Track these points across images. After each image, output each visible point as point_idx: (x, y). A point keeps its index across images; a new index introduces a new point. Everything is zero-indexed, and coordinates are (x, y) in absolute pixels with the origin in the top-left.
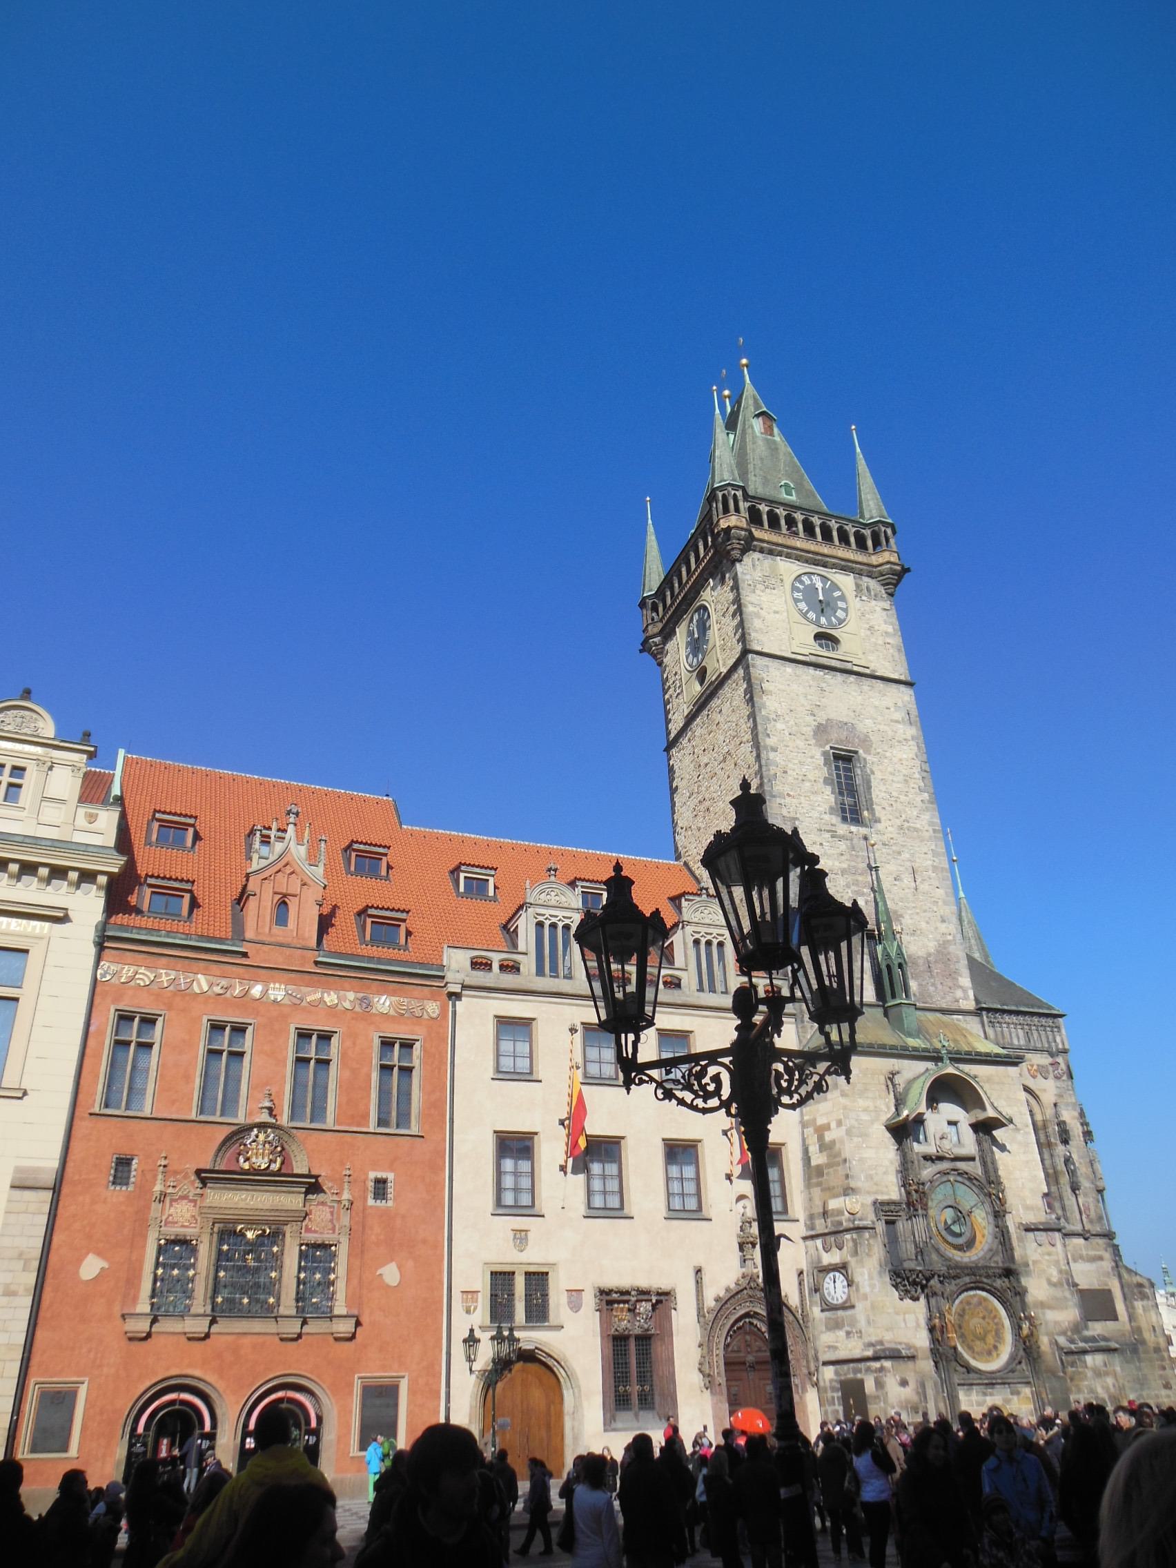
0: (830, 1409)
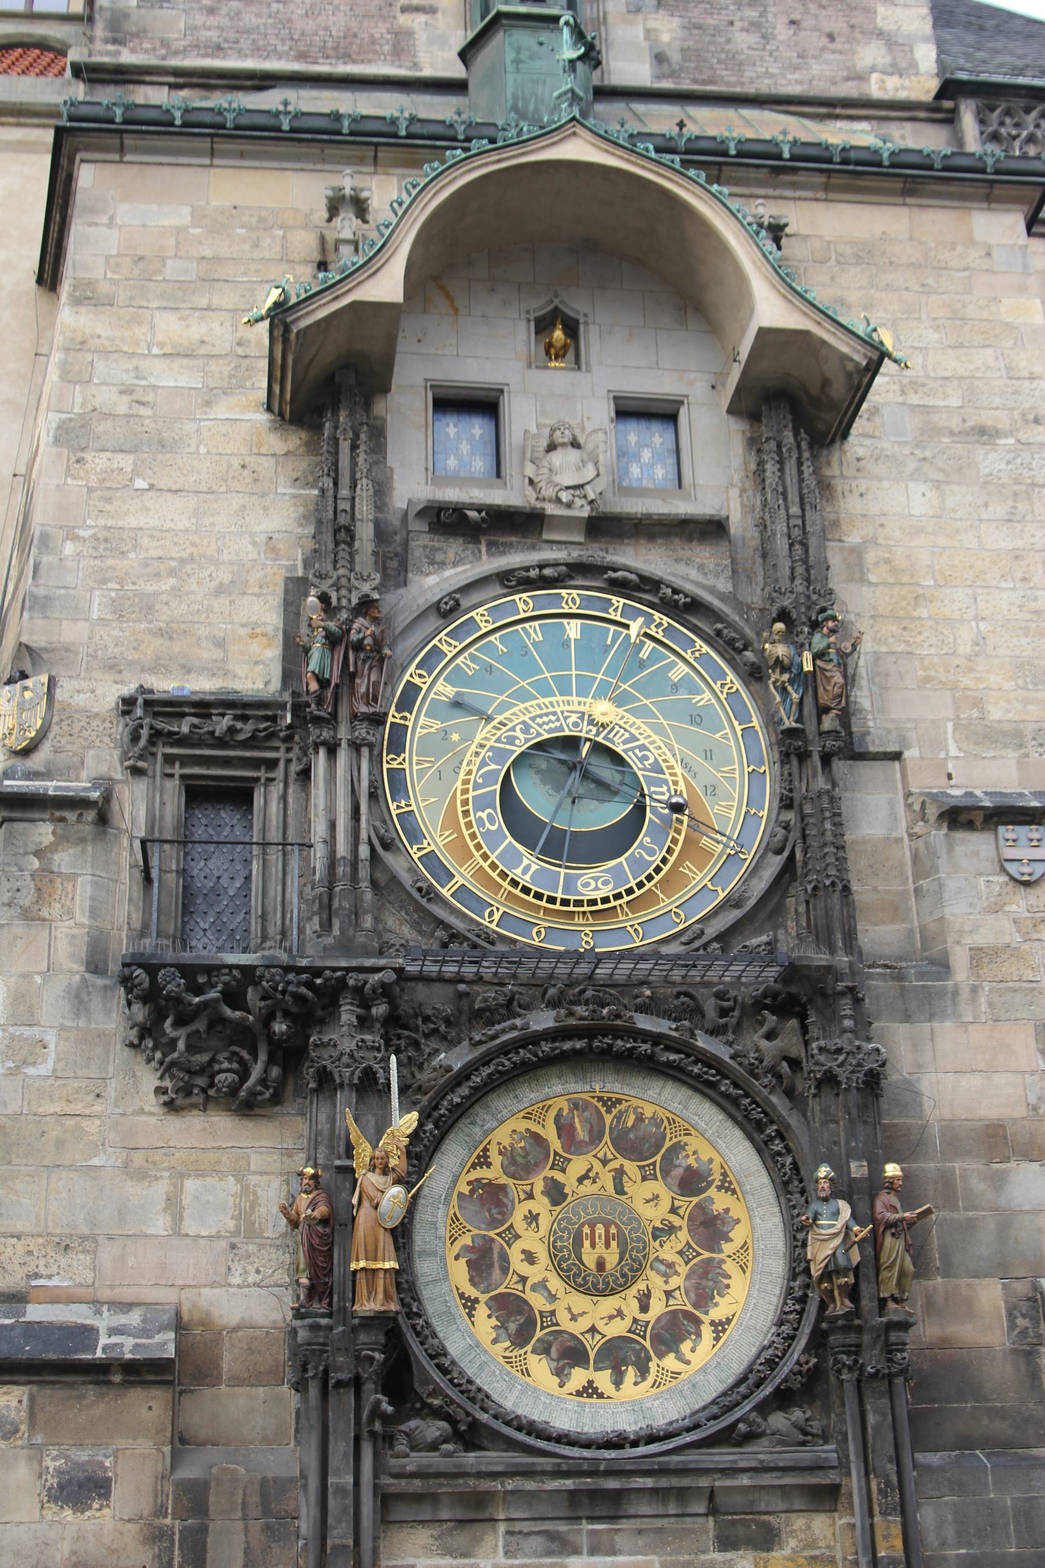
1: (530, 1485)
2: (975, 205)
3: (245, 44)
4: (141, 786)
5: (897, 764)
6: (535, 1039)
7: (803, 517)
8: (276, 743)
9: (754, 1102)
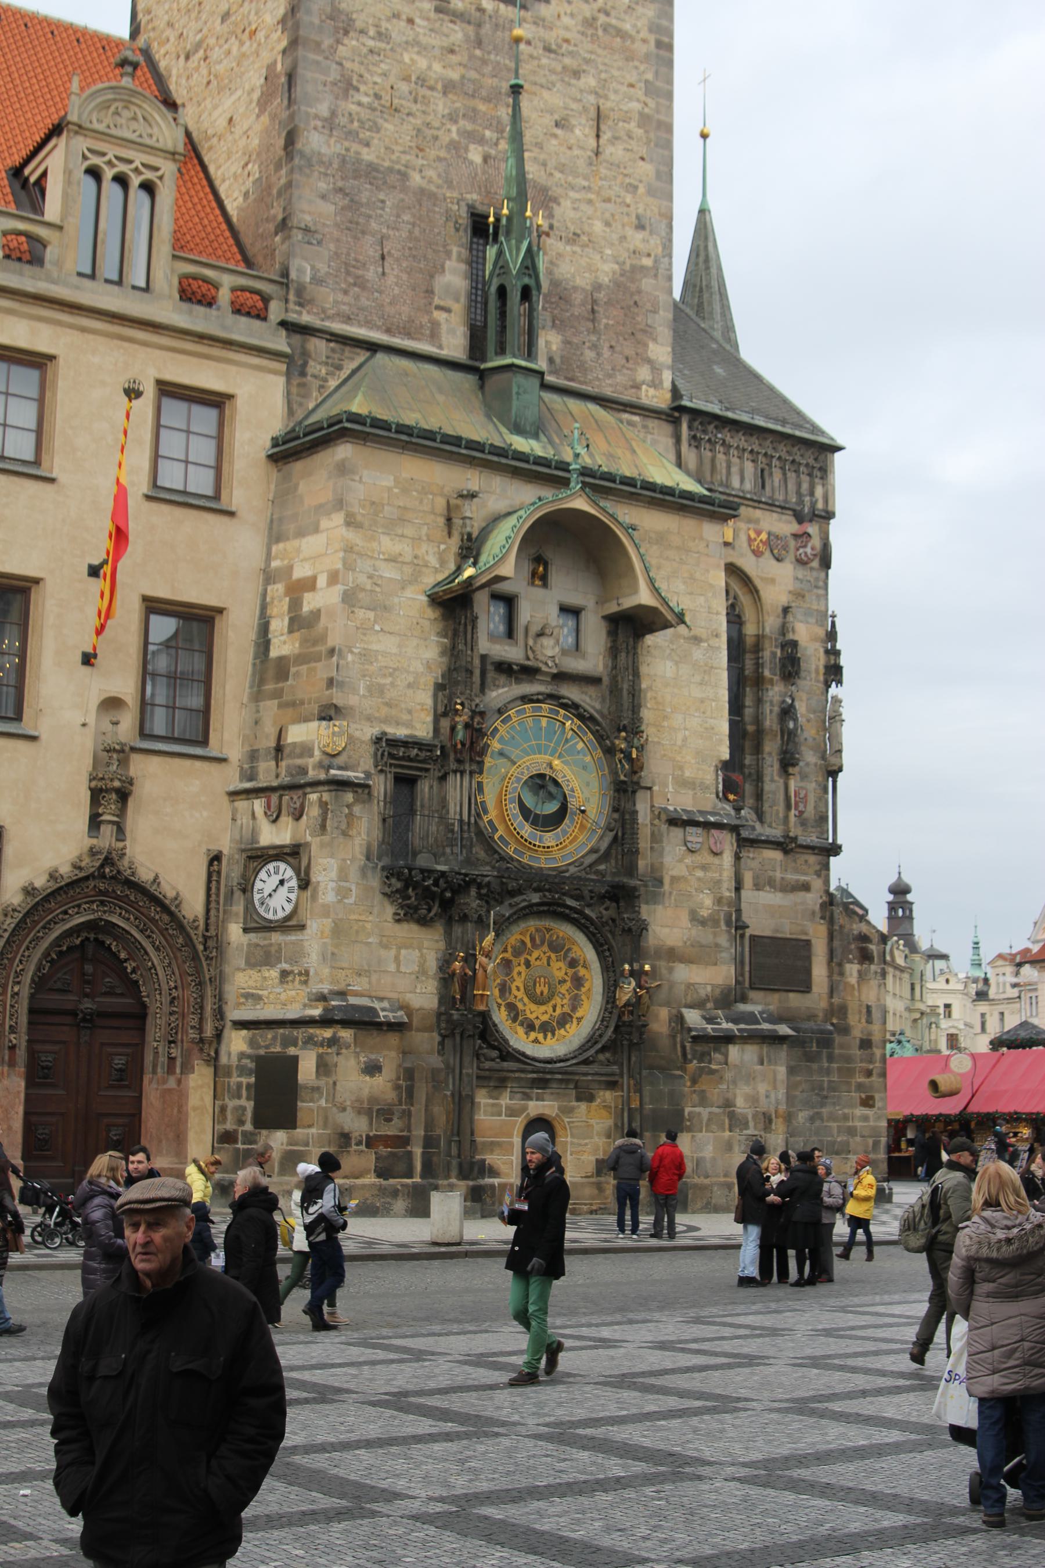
0: (231, 1104)
1: (523, 1075)
3: (361, 318)
4: (382, 777)
6: (532, 905)
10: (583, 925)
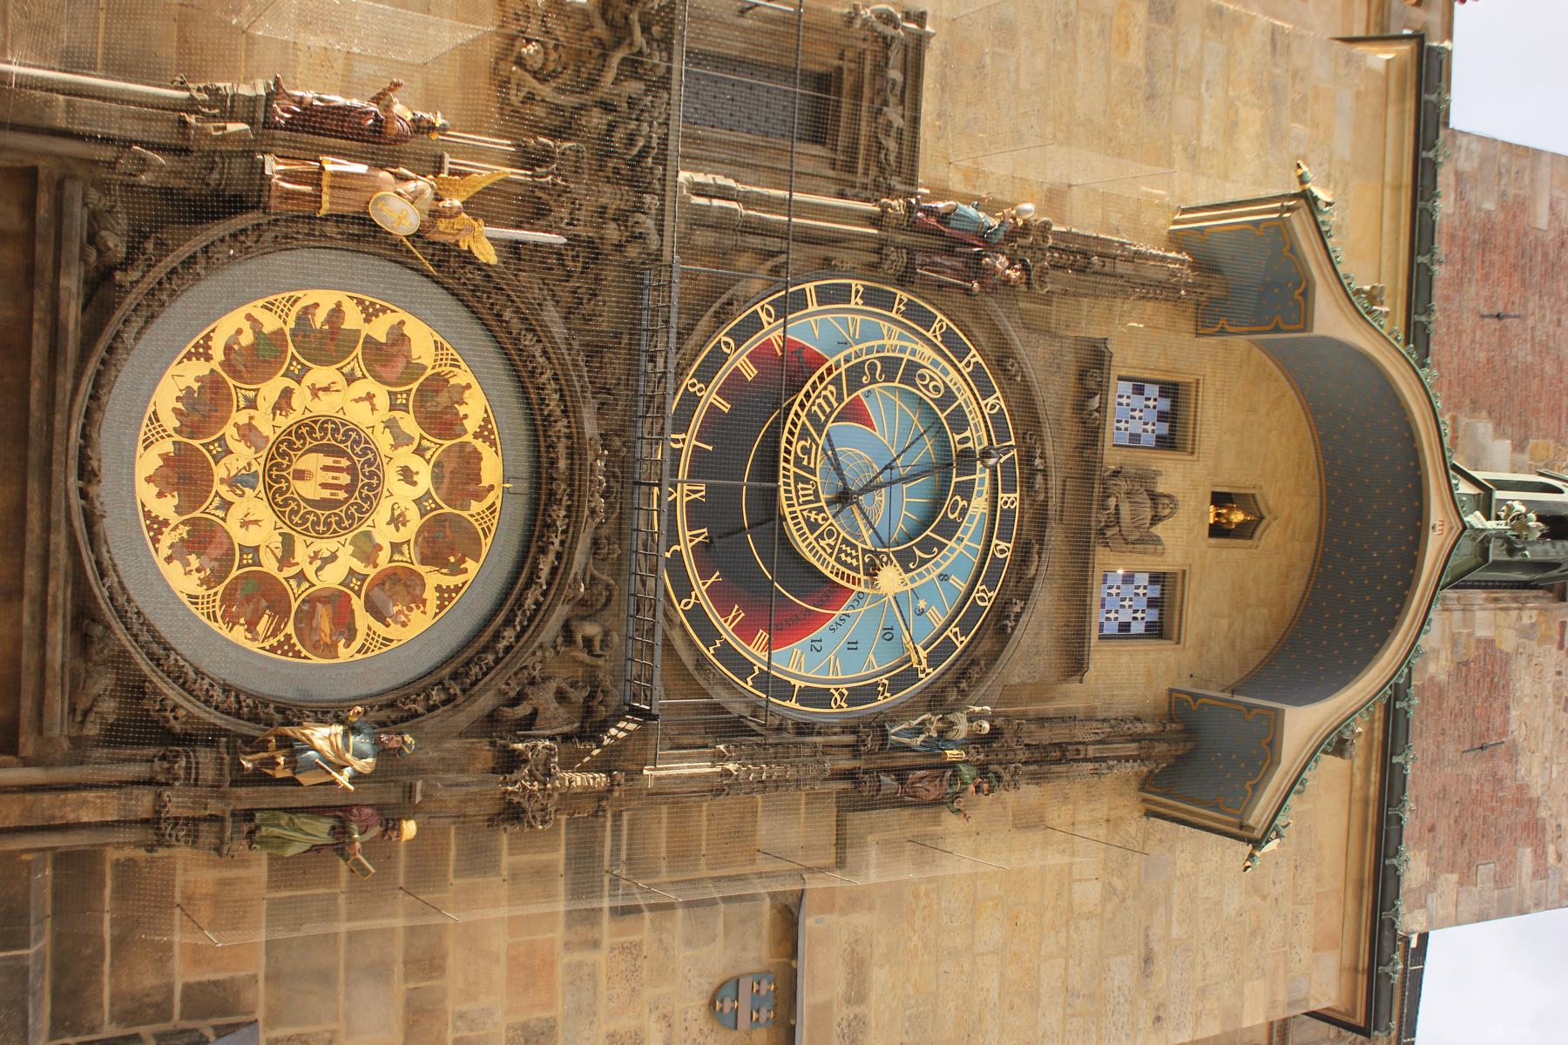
2: (1345, 955)
5: (832, 860)
7: (1086, 760)
8: (873, 171)
9: (490, 669)
10: (519, 602)
